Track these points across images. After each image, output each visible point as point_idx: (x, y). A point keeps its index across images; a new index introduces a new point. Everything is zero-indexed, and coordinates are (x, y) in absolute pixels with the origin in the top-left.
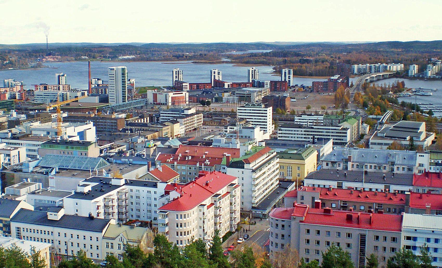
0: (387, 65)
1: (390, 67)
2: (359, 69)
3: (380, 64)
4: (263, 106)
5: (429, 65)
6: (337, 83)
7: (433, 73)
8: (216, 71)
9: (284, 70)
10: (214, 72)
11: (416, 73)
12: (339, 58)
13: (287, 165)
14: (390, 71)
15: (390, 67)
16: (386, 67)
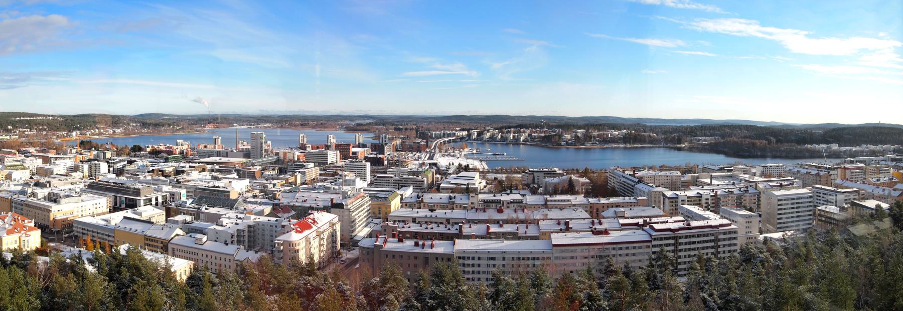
2: (435, 135)
4: (364, 162)
8: (332, 136)
9: (381, 136)
10: (330, 137)
12: (422, 127)
13: (378, 206)
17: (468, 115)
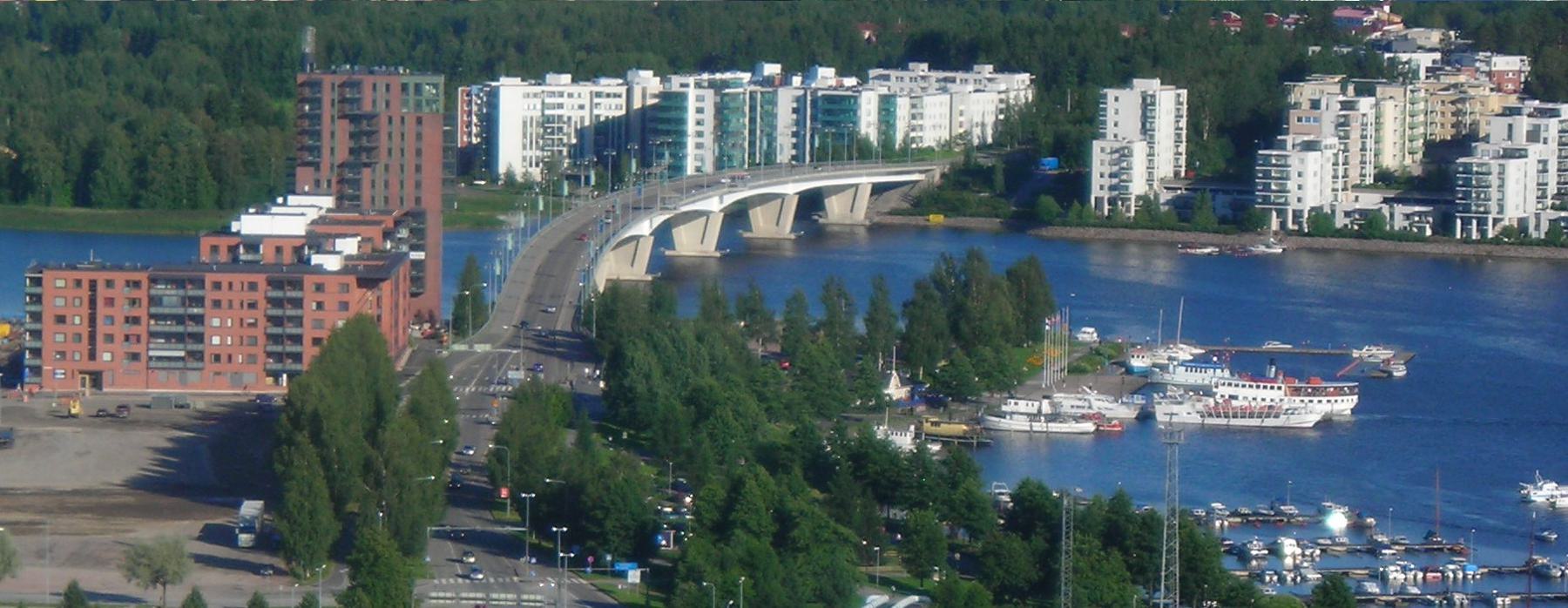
0: (850, 81)
3: (772, 69)
5: (1304, 92)
6: (309, 281)
7: (1354, 177)
11: (1165, 169)
14: (889, 153)
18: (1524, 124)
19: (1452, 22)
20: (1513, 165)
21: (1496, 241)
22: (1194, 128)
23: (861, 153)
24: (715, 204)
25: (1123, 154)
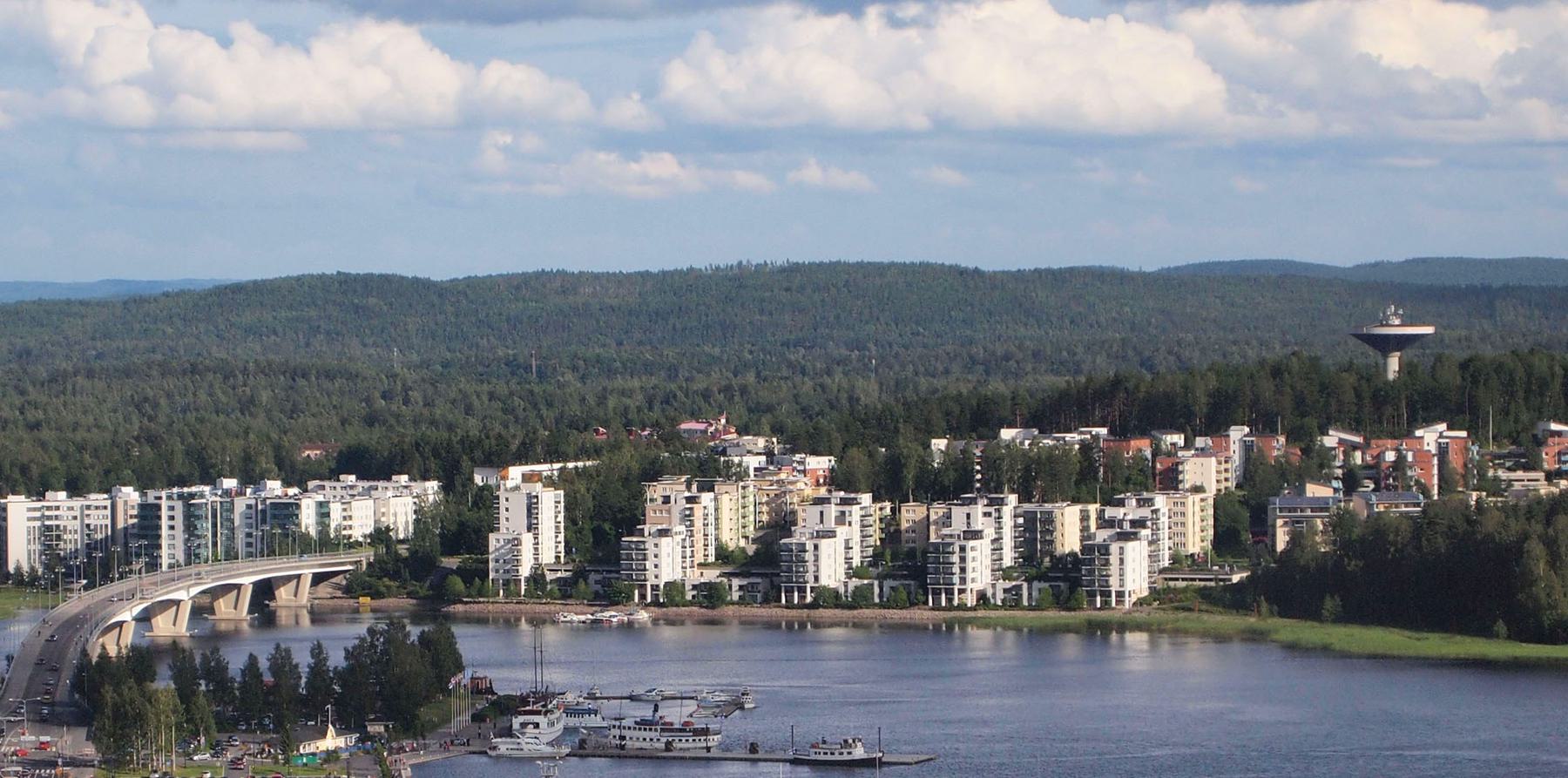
0: (293, 491)
1: (323, 513)
3: (230, 483)
5: (656, 491)
7: (699, 558)
11: (548, 557)
14: (326, 543)
15: (323, 513)
16: (285, 513)
17: (440, 271)
18: (832, 511)
19: (777, 430)
20: (825, 544)
21: (814, 605)
22: (571, 520)
23: (305, 546)
24: (186, 594)
25: (516, 542)
